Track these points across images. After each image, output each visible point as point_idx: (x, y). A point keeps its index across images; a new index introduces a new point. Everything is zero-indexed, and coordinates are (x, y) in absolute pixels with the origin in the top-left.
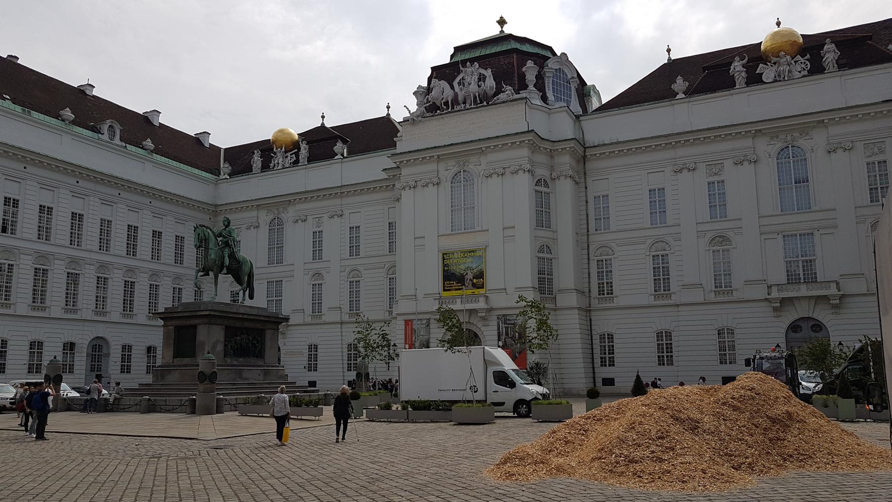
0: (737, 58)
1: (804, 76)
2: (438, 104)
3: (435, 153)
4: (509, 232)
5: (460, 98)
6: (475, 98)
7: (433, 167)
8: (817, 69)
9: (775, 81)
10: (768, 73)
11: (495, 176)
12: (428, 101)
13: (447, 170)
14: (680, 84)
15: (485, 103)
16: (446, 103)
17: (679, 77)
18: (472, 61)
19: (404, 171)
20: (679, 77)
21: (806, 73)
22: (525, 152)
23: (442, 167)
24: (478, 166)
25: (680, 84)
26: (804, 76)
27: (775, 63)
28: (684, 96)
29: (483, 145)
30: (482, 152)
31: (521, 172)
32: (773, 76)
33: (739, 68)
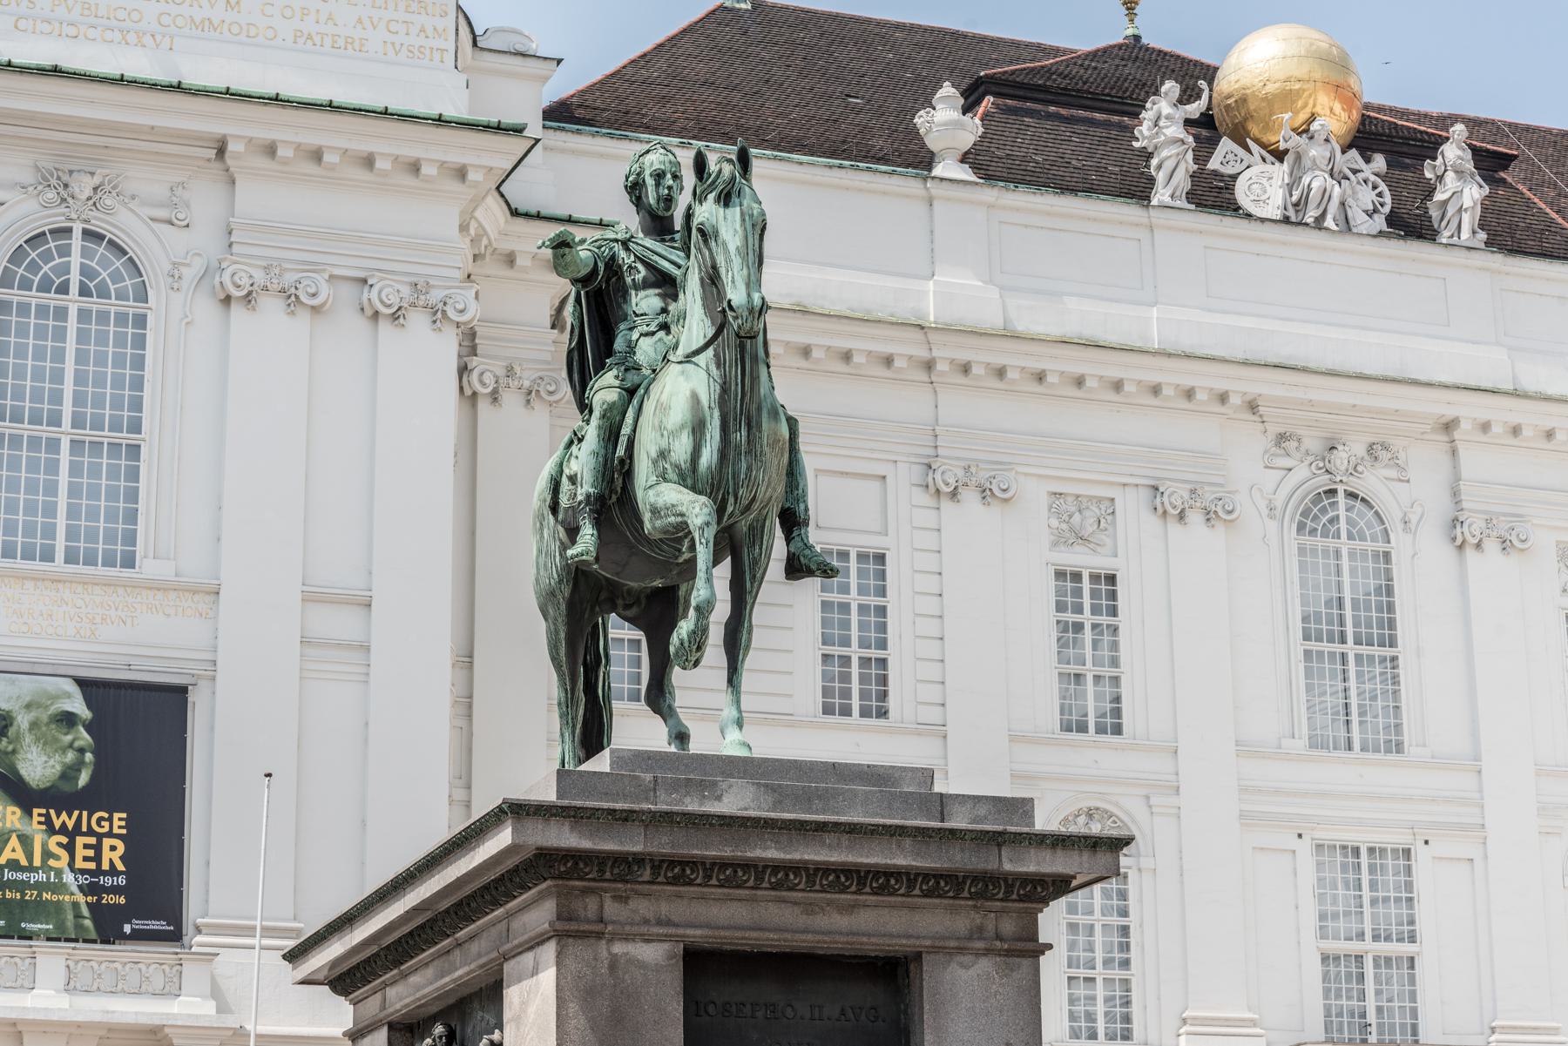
0: (1171, 87)
1: (1381, 234)
4: (339, 624)
8: (1411, 223)
9: (1286, 220)
10: (1262, 186)
11: (271, 307)
14: (946, 122)
20: (947, 90)
21: (1379, 222)
25: (946, 122)
26: (1381, 234)
27: (1280, 156)
28: (964, 173)
31: (418, 321)
32: (1280, 202)
33: (1175, 130)
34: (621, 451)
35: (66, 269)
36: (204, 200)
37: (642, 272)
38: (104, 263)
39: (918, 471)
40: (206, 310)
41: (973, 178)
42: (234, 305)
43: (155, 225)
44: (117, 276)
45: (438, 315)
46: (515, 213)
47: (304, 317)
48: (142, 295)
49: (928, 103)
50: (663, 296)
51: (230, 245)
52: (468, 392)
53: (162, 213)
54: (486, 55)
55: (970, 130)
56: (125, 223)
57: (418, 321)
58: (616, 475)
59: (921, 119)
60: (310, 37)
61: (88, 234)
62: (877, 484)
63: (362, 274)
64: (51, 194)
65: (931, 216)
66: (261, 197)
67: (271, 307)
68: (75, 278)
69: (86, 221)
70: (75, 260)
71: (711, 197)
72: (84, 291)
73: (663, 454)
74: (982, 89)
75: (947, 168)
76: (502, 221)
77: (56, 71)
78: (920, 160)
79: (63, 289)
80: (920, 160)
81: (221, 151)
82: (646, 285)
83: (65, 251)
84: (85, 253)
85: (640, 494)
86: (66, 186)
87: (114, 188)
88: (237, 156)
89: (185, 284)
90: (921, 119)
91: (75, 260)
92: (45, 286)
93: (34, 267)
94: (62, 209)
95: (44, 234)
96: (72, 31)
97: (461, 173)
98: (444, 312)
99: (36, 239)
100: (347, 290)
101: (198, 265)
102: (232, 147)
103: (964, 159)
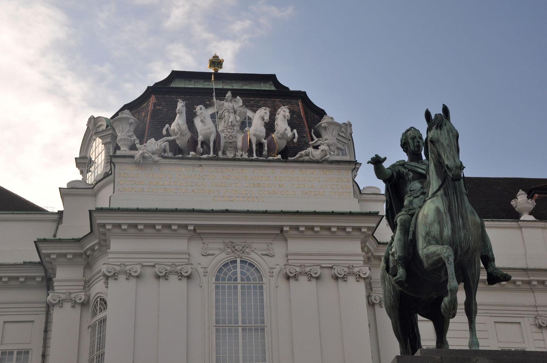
2: (182, 142)
3: (192, 221)
5: (222, 144)
6: (260, 145)
7: (179, 245)
11: (303, 279)
12: (168, 134)
13: (206, 257)
14: (522, 201)
15: (279, 156)
16: (205, 143)
17: (521, 192)
18: (235, 93)
19: (117, 245)
20: (521, 192)
22: (355, 247)
23: (196, 248)
24: (269, 257)
25: (522, 201)
28: (532, 218)
29: (286, 222)
30: (281, 233)
31: (351, 279)
34: (410, 237)
35: (236, 273)
36: (278, 248)
37: (411, 175)
38: (248, 270)
39: (532, 320)
40: (282, 282)
41: (534, 219)
42: (291, 280)
43: (263, 257)
44: (252, 274)
45: (359, 277)
46: (379, 243)
47: (314, 281)
48: (261, 279)
49: (515, 197)
50: (421, 183)
51: (288, 260)
52: (371, 303)
53: (266, 252)
54: (365, 196)
55: (531, 204)
56: (254, 257)
57: (351, 279)
58: (410, 245)
59: (513, 203)
60: (306, 193)
61: (242, 262)
62: (518, 325)
63: (331, 266)
64: (229, 250)
65: (522, 233)
66: (296, 246)
67: (303, 279)
68: (239, 275)
69: (241, 258)
70: (239, 270)
71: (434, 128)
72: (242, 280)
73: (428, 234)
74: (533, 192)
75: (526, 217)
76: (375, 246)
77: (227, 211)
78: (515, 215)
79: (236, 279)
80: (515, 215)
81: (282, 231)
82: (414, 179)
83: (235, 267)
84: (242, 267)
85: (420, 252)
86: (234, 247)
87: (249, 246)
88: (287, 231)
89: (274, 274)
90: (513, 203)
91: (239, 270)
92: (230, 279)
93: (225, 274)
94: (233, 254)
95: (228, 263)
96: (231, 199)
97: (359, 229)
98: (359, 275)
99: (226, 265)
100: (327, 272)
101: (278, 268)
102: (285, 229)
103: (531, 214)
